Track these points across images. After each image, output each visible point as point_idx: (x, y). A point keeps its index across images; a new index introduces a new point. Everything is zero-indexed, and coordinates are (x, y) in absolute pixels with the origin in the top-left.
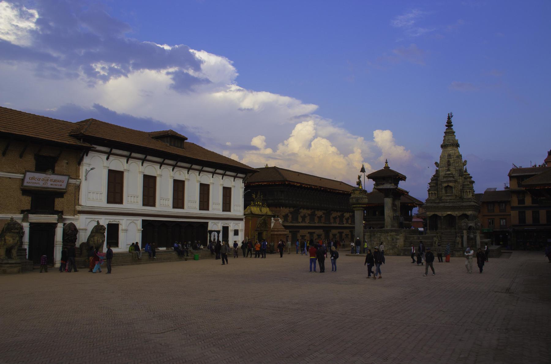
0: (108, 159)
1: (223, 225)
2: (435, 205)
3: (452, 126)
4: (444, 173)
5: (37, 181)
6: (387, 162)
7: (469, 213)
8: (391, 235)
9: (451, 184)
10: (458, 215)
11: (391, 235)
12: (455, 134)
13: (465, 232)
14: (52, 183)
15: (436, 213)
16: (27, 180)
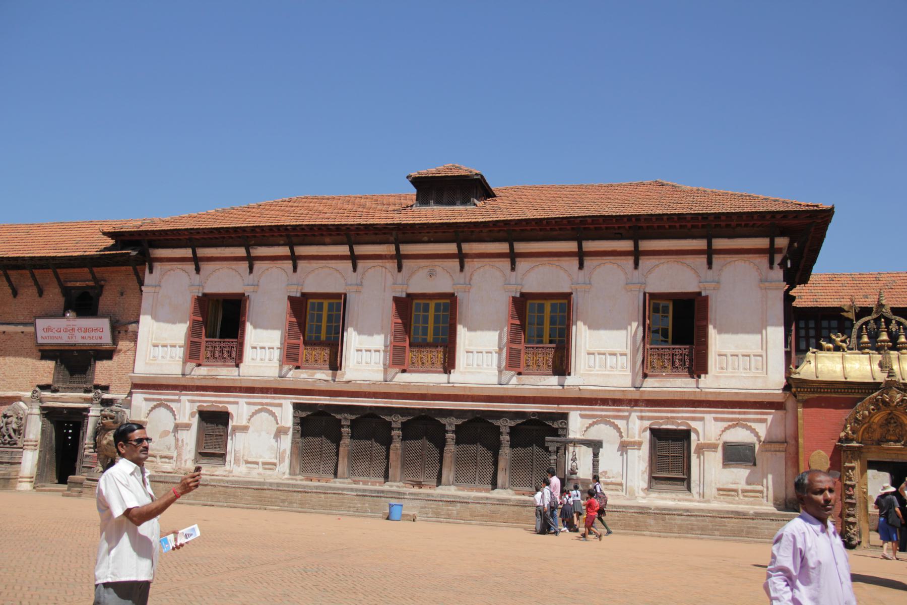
0: (198, 270)
1: (647, 423)
5: (57, 334)
14: (83, 334)
16: (40, 333)
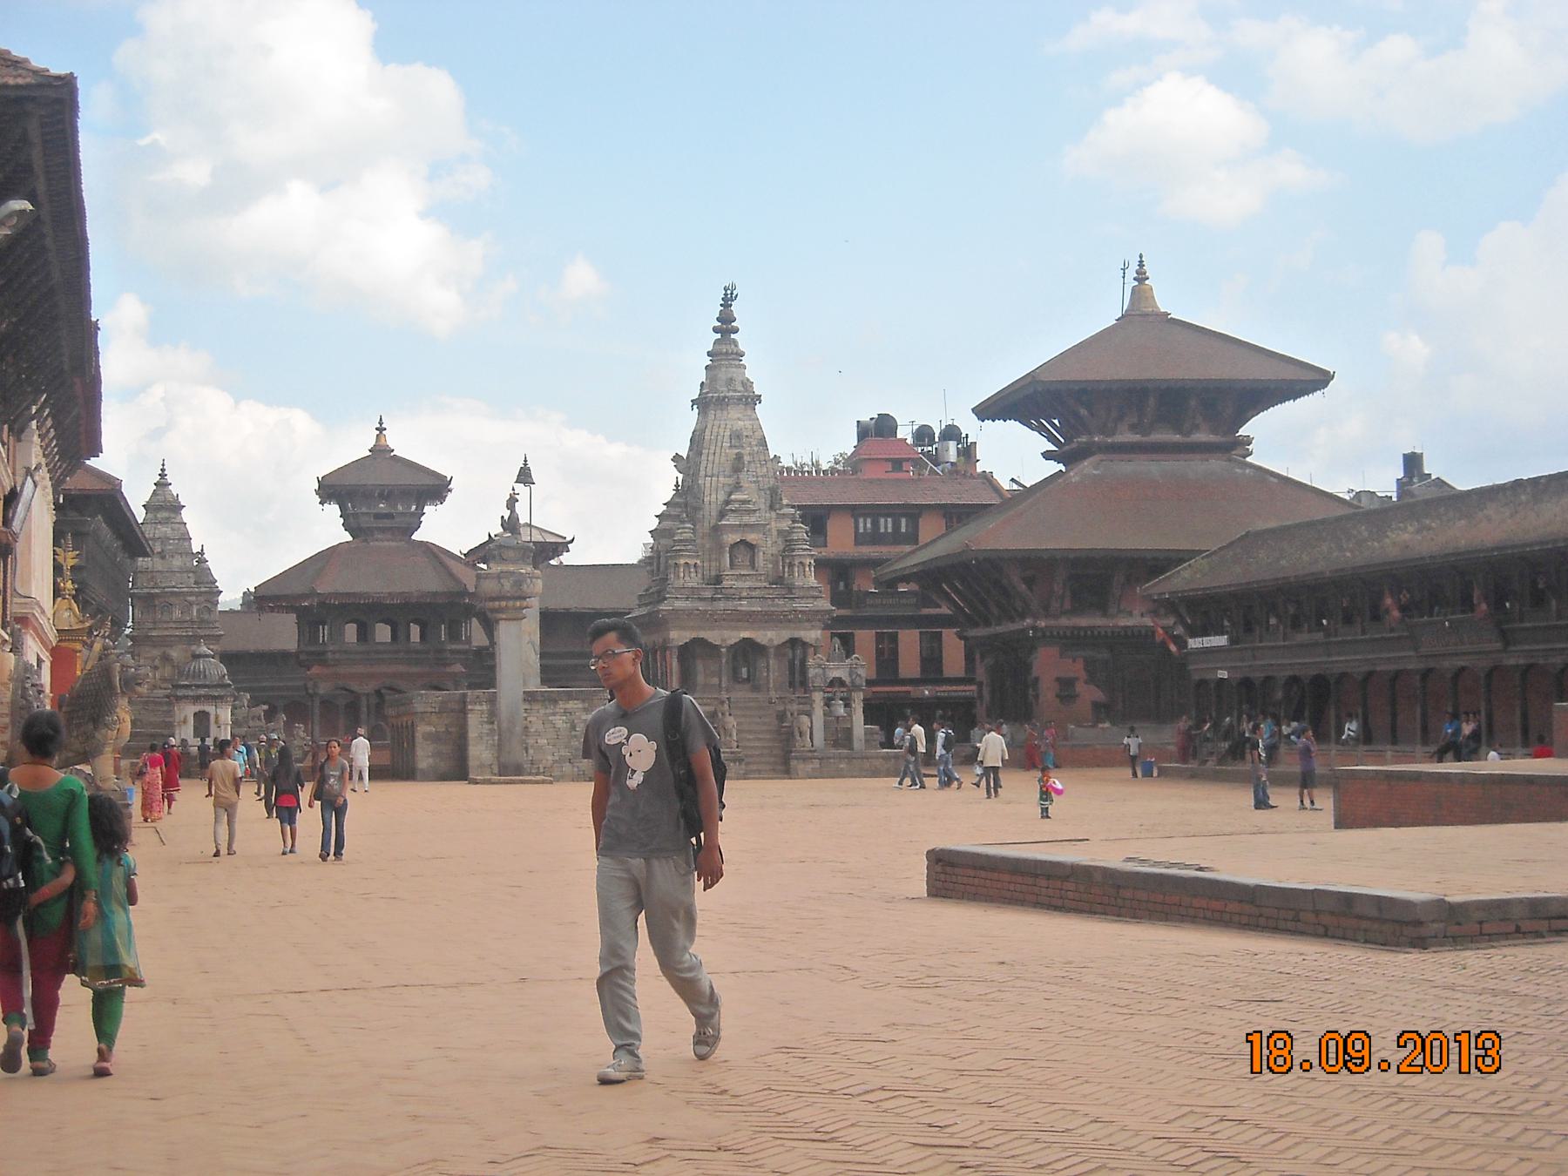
2: (701, 606)
3: (736, 331)
4: (722, 497)
6: (381, 429)
7: (812, 635)
8: (566, 712)
9: (751, 537)
10: (776, 643)
11: (566, 712)
12: (745, 361)
13: (818, 697)
15: (702, 634)
